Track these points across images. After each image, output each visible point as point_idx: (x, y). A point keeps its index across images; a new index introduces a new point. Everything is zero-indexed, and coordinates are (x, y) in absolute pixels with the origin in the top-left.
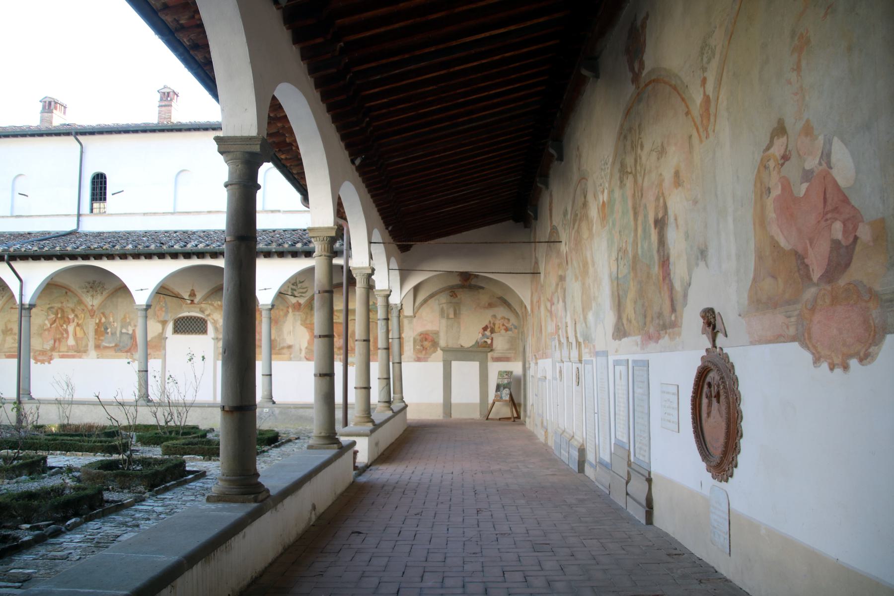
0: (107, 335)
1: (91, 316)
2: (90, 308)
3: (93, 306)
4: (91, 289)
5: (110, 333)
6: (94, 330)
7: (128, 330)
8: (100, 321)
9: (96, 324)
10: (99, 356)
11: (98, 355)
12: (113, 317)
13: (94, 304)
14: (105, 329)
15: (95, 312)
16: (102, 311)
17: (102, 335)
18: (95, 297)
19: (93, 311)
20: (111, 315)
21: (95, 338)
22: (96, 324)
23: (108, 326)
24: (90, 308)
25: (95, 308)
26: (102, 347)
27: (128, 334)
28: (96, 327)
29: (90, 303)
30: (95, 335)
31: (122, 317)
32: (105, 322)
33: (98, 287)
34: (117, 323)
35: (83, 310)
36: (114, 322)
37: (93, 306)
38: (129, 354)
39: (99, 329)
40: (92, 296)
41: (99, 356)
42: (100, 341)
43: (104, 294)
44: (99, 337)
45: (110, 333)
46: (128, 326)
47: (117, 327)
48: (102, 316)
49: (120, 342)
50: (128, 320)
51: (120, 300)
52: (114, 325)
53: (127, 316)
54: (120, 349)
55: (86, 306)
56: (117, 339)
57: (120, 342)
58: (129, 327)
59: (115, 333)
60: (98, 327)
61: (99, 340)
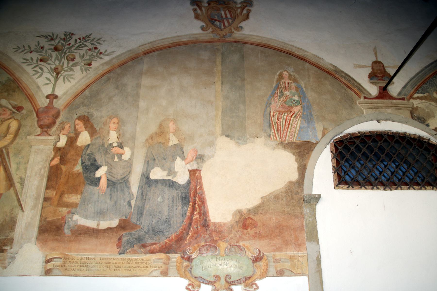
0: (92, 188)
1: (41, 127)
2: (43, 102)
3: (52, 97)
4: (54, 54)
5: (103, 182)
6: (45, 172)
7: (171, 172)
8: (72, 141)
9: (57, 150)
10: (50, 266)
11: (48, 261)
12: (117, 129)
13: (58, 92)
14: (85, 168)
15: (58, 115)
16: (82, 111)
17: (75, 190)
18: (64, 73)
19: (53, 112)
20: (113, 126)
21: (46, 199)
22: (57, 150)
23: (100, 159)
24: (43, 102)
25: (59, 104)
26: (67, 231)
27: (172, 184)
28: (56, 161)
29: (48, 90)
30: (47, 188)
31: (153, 129)
32: (88, 146)
33: (78, 48)
34: (132, 149)
35: (19, 109)
36: (121, 146)
37: (52, 97)
38: (175, 257)
39: (64, 168)
40: (57, 72)
41: (50, 266)
42: (64, 210)
43: (94, 64)
44: (62, 194)
45: (103, 182)
46: (174, 159)
47: (129, 164)
48: (80, 125)
49: (140, 212)
50: (173, 141)
51: (146, 81)
52: (120, 156)
53: (172, 126)
54: (139, 239)
55: (30, 98)
56: (129, 203)
57: (140, 212)
58: (179, 163)
59: (125, 182)
60: (63, 160)
61: (61, 204)
